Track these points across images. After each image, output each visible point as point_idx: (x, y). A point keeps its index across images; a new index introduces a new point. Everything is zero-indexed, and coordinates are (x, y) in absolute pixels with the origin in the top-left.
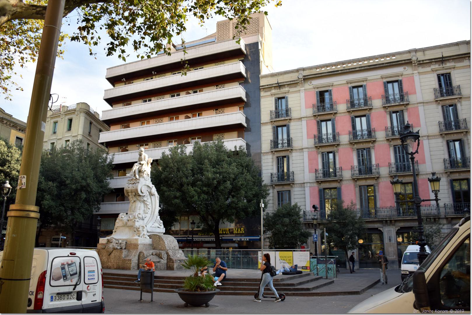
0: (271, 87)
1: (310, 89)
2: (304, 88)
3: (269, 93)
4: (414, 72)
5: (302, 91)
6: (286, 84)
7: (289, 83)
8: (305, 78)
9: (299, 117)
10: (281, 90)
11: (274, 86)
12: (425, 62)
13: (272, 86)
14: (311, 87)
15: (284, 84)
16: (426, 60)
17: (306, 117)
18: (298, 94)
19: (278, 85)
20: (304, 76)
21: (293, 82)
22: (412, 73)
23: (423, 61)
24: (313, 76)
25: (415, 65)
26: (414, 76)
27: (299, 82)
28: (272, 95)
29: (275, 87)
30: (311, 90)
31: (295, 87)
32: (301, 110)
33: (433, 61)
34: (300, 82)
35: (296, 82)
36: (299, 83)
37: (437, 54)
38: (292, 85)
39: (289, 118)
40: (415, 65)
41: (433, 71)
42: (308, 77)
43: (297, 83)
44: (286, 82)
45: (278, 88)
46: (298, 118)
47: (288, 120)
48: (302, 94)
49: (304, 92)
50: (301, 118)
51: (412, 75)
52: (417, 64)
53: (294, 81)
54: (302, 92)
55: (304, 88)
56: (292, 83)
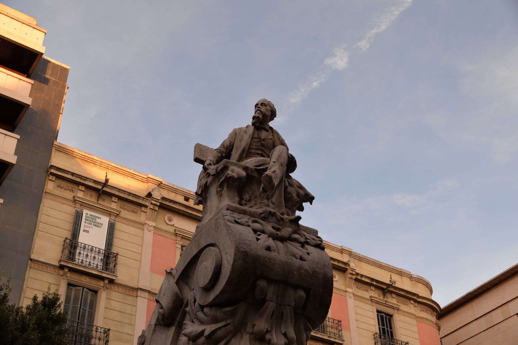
0: (78, 184)
1: (168, 232)
2: (154, 224)
3: (69, 195)
4: (348, 289)
5: (150, 228)
6: (117, 193)
7: (126, 196)
8: (164, 202)
9: (134, 285)
10: (100, 202)
11: (87, 183)
12: (363, 279)
13: (82, 181)
14: (172, 229)
15: (113, 192)
16: (366, 277)
17: (149, 292)
18: (138, 231)
19: (100, 187)
20: (163, 198)
21: (135, 200)
22: (343, 288)
23: (362, 276)
24: (181, 208)
25: (351, 278)
26: (348, 297)
27: (147, 204)
28: (75, 201)
29: (88, 187)
30: (167, 235)
31: (133, 212)
32: (139, 270)
33: (374, 283)
34: (152, 207)
35: (140, 201)
36: (146, 207)
37: (384, 277)
38: (127, 205)
39: (110, 277)
40: (351, 278)
41: (372, 300)
42: (171, 205)
43: (141, 205)
44: (119, 190)
45: (94, 194)
46: (130, 285)
47: (106, 281)
48: (149, 236)
49: (152, 232)
50: (138, 289)
51: (344, 294)
52: (354, 277)
53: (139, 197)
54: (149, 231)
55: (154, 224)
56: (131, 198)
